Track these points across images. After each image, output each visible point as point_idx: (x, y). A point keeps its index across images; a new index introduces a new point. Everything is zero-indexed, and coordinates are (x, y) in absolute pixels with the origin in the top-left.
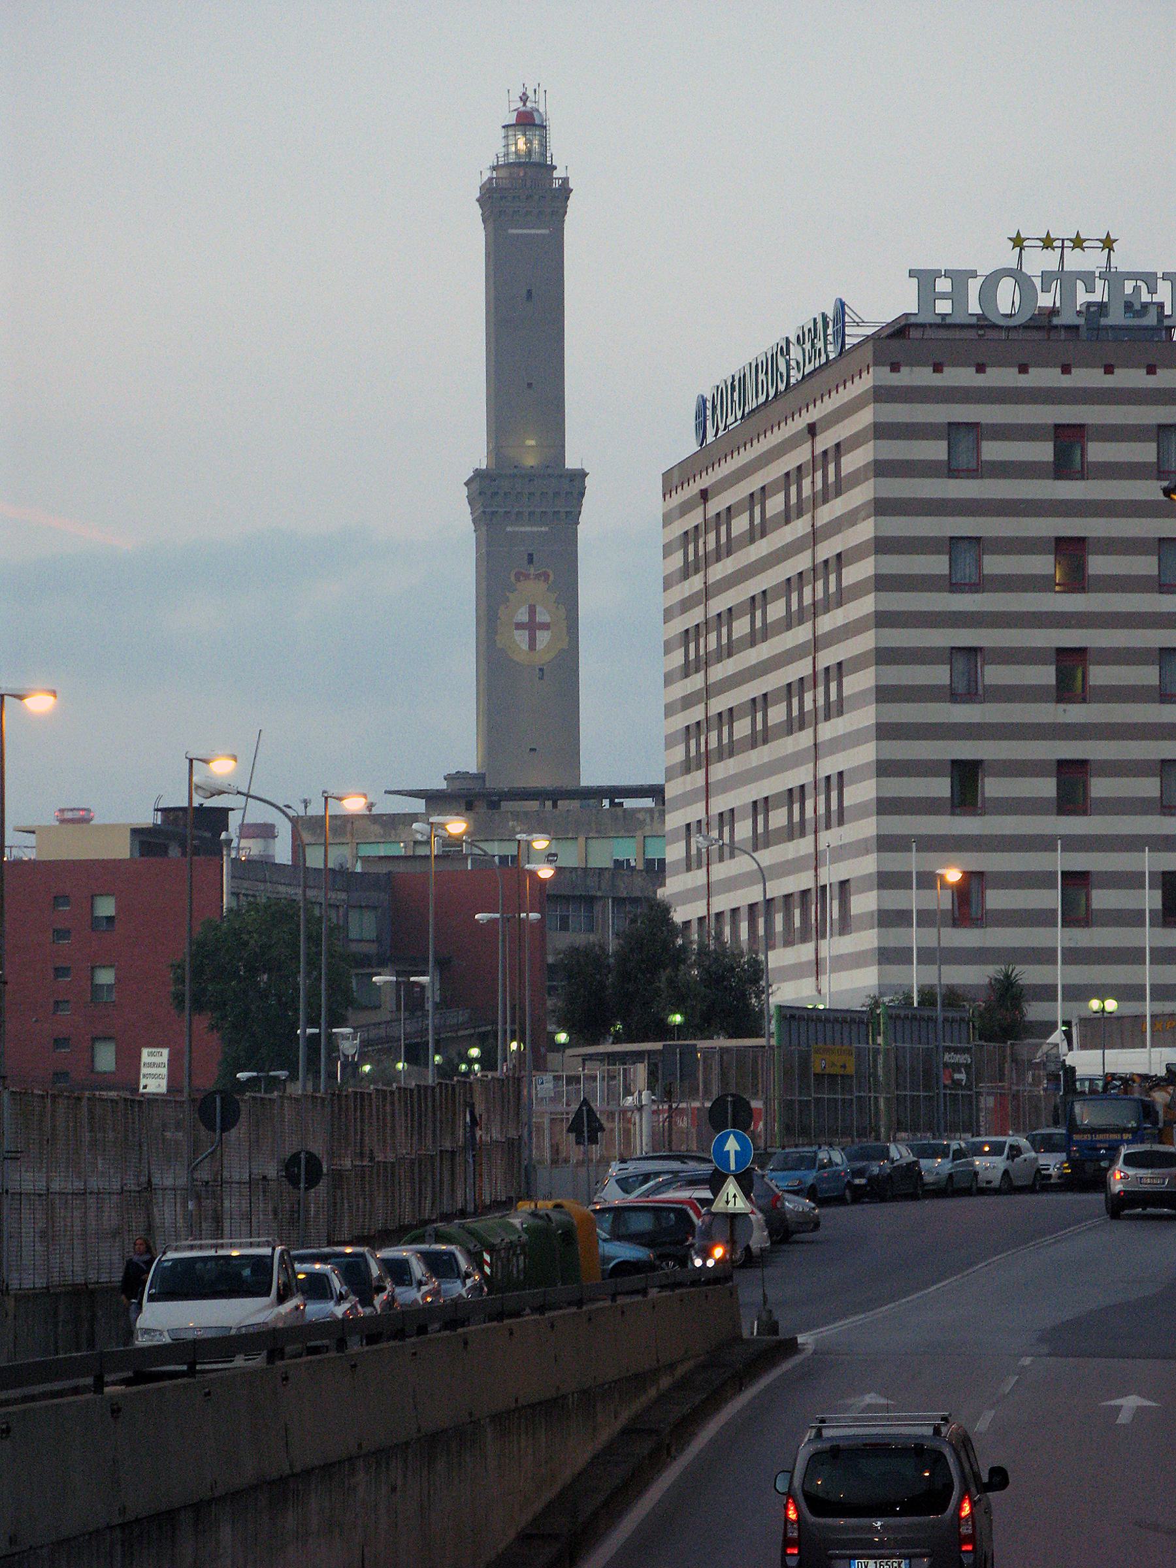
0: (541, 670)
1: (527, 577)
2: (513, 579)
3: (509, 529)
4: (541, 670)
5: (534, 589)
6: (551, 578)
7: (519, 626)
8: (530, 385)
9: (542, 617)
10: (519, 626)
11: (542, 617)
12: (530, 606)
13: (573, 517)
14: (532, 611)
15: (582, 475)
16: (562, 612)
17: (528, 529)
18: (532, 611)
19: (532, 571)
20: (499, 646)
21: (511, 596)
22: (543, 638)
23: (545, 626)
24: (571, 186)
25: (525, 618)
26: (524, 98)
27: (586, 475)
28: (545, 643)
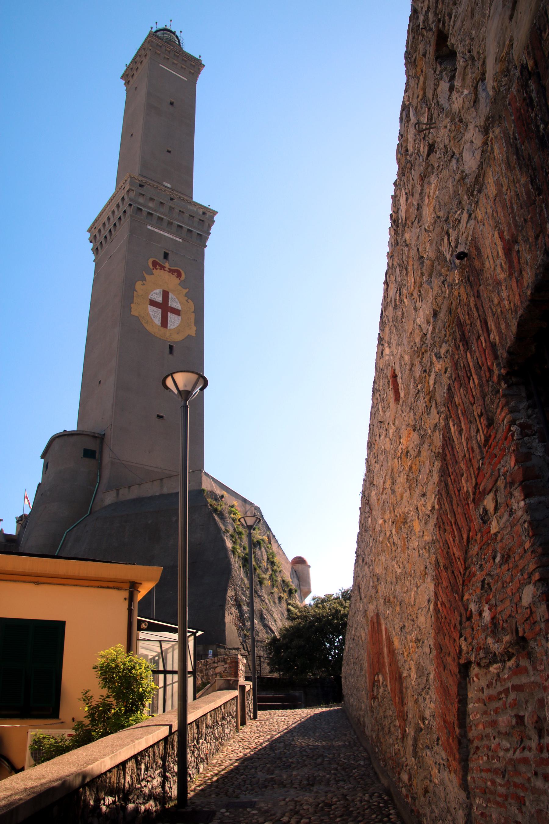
0: (171, 347)
1: (163, 268)
3: (149, 227)
4: (171, 347)
7: (153, 303)
10: (153, 303)
11: (174, 303)
12: (164, 291)
13: (202, 239)
14: (165, 295)
16: (191, 305)
17: (166, 234)
18: (165, 295)
19: (167, 265)
20: (134, 312)
22: (174, 321)
23: (177, 312)
24: (203, 63)
25: (159, 299)
27: (215, 213)
28: (176, 325)
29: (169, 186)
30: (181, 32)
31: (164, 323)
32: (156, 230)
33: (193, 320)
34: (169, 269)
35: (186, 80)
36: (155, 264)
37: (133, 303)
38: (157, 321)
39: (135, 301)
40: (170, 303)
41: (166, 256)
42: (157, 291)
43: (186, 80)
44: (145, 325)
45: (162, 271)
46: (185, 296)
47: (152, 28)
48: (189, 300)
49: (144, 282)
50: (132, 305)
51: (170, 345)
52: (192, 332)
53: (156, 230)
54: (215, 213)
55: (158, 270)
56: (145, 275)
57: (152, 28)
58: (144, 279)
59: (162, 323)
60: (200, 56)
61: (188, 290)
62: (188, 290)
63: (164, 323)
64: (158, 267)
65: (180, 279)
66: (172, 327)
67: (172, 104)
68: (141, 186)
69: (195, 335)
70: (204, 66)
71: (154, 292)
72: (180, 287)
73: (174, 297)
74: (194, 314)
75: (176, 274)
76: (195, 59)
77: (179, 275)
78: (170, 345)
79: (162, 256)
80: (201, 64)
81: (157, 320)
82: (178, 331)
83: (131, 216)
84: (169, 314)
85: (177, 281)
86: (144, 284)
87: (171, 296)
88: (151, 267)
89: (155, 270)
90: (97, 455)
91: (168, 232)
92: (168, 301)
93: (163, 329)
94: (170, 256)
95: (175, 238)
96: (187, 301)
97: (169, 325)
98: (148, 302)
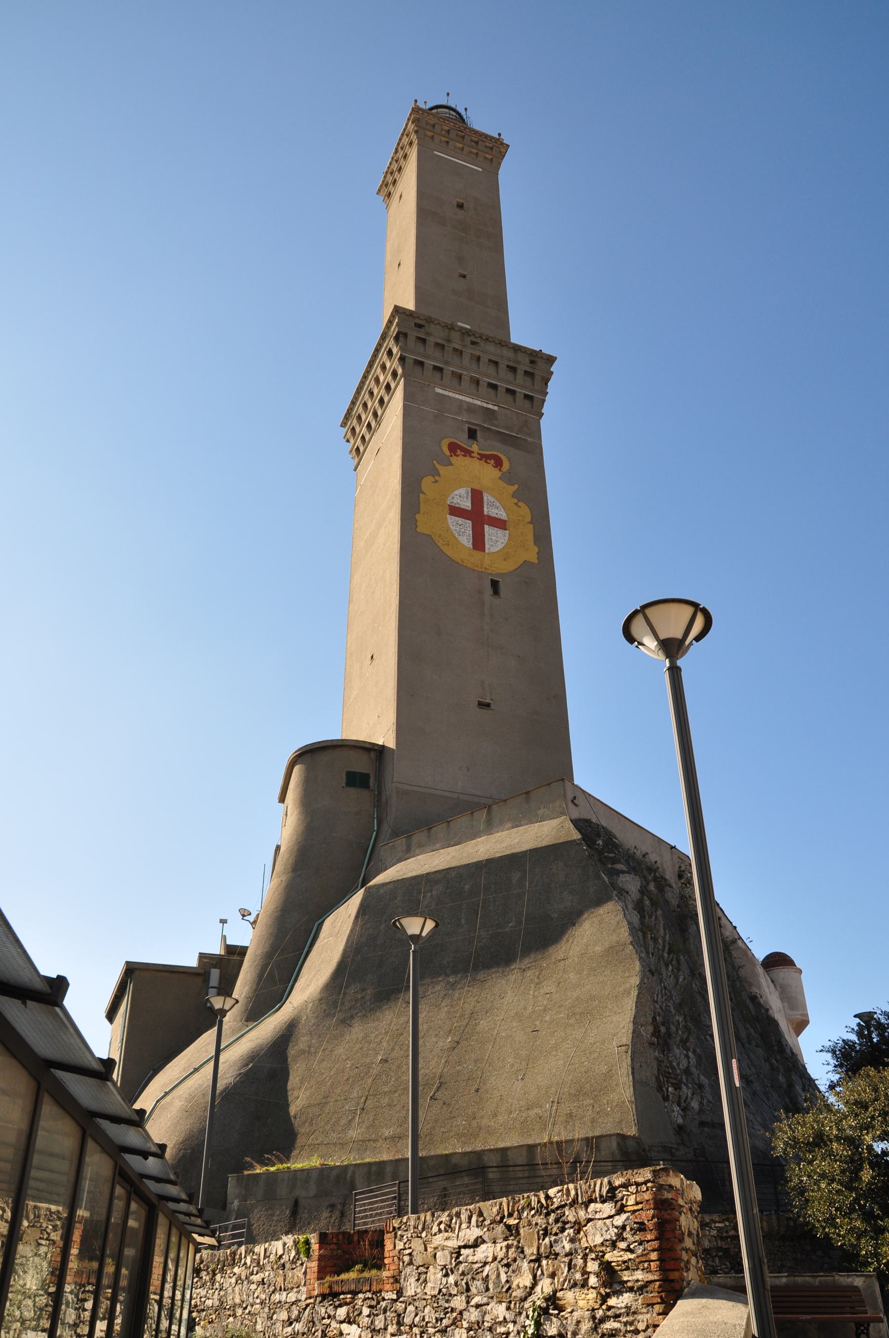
0: (495, 584)
1: (468, 453)
3: (439, 390)
6: (506, 466)
7: (455, 511)
10: (455, 511)
12: (473, 491)
13: (534, 403)
14: (477, 497)
16: (525, 512)
18: (477, 497)
19: (475, 448)
21: (442, 469)
23: (499, 524)
25: (467, 504)
28: (500, 546)
30: (466, 109)
31: (479, 542)
32: (451, 394)
33: (530, 537)
34: (478, 454)
37: (419, 513)
38: (466, 540)
39: (422, 512)
40: (485, 510)
41: (472, 434)
42: (462, 491)
44: (445, 549)
45: (468, 458)
46: (513, 496)
47: (416, 101)
48: (521, 504)
49: (437, 478)
50: (417, 516)
51: (492, 581)
52: (532, 554)
53: (451, 394)
54: (551, 360)
55: (461, 458)
56: (438, 466)
57: (416, 101)
59: (473, 544)
60: (499, 135)
61: (516, 486)
62: (516, 486)
63: (479, 542)
64: (459, 452)
65: (500, 470)
66: (493, 550)
67: (460, 206)
68: (420, 326)
69: (536, 561)
70: (508, 146)
71: (456, 492)
72: (502, 484)
73: (492, 499)
74: (531, 526)
75: (492, 462)
76: (492, 138)
77: (498, 463)
78: (492, 581)
79: (465, 435)
80: (502, 144)
81: (465, 538)
82: (504, 554)
83: (404, 375)
84: (486, 527)
85: (496, 473)
86: (436, 481)
87: (486, 497)
88: (448, 453)
89: (454, 457)
90: (372, 781)
92: (483, 507)
93: (478, 554)
95: (485, 405)
96: (516, 504)
97: (487, 546)
98: (447, 509)
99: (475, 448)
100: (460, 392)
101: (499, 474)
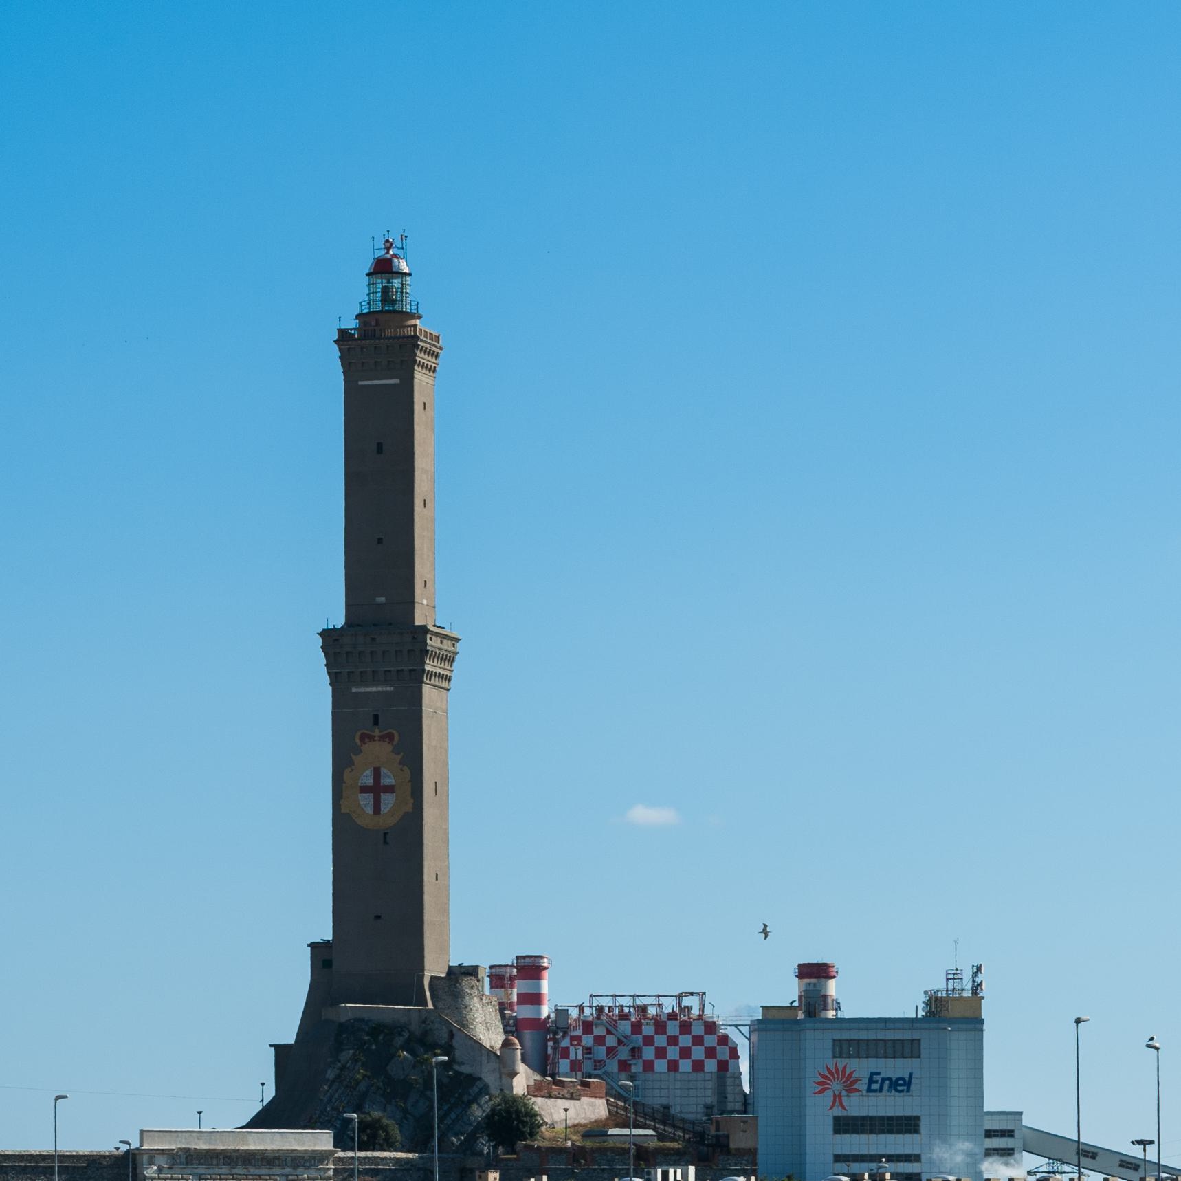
0: (385, 834)
1: (372, 738)
2: (358, 741)
5: (379, 751)
7: (364, 789)
8: (380, 541)
9: (387, 781)
10: (364, 789)
11: (387, 781)
14: (377, 773)
15: (424, 630)
17: (374, 689)
18: (377, 773)
22: (388, 801)
23: (390, 789)
25: (370, 782)
26: (389, 245)
29: (382, 600)
31: (377, 809)
32: (362, 690)
35: (397, 381)
36: (363, 738)
38: (370, 810)
43: (397, 381)
44: (358, 821)
48: (405, 768)
53: (362, 690)
58: (351, 763)
63: (377, 809)
85: (390, 748)
87: (383, 771)
91: (376, 685)
94: (381, 720)
99: (377, 732)
100: (367, 686)
101: (390, 748)
